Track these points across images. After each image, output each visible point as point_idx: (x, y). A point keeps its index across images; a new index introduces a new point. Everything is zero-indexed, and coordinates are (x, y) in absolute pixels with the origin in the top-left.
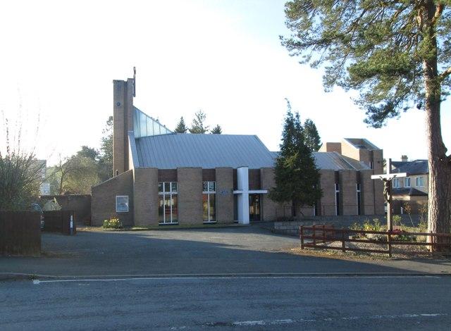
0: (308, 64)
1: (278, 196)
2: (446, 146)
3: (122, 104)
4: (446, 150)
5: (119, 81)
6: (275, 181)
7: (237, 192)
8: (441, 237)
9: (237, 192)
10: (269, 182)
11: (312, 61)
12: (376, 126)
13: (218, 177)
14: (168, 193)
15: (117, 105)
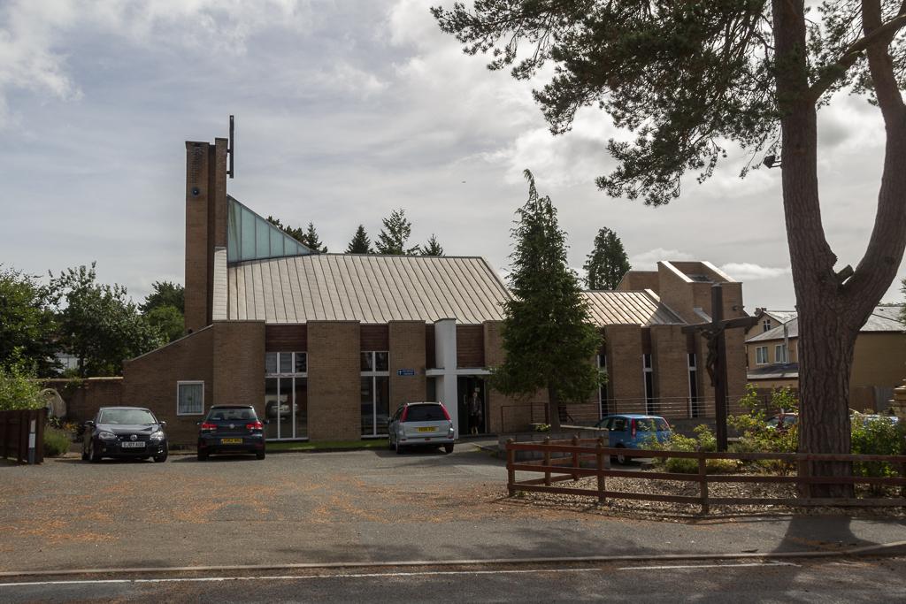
0: (509, 68)
1: (514, 381)
2: (833, 250)
3: (204, 188)
4: (834, 259)
5: (198, 144)
6: (154, 292)
7: (432, 372)
8: (829, 462)
9: (432, 372)
10: (497, 354)
11: (516, 63)
12: (656, 200)
13: (393, 341)
14: (286, 375)
15: (193, 194)
